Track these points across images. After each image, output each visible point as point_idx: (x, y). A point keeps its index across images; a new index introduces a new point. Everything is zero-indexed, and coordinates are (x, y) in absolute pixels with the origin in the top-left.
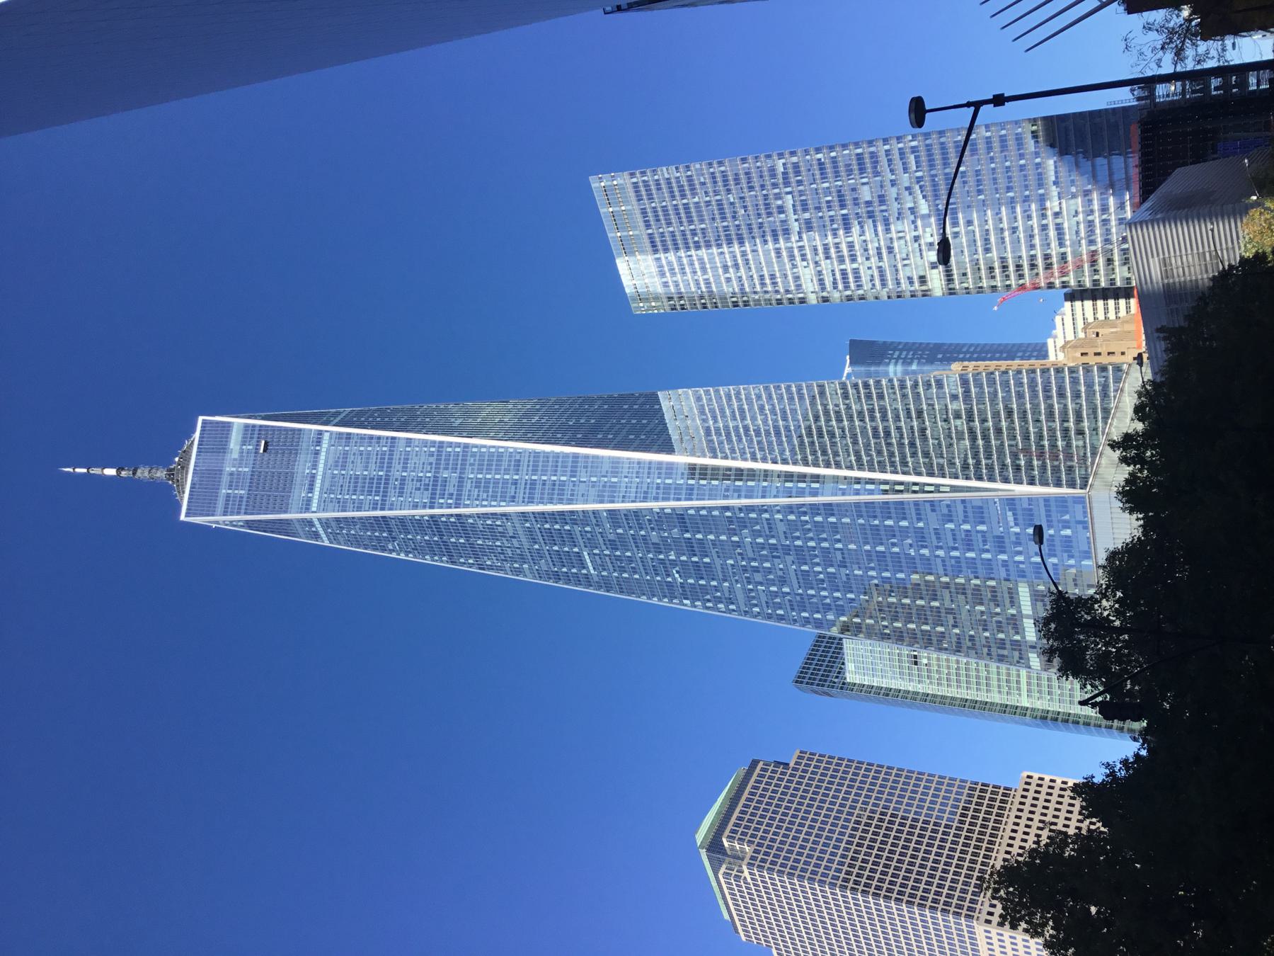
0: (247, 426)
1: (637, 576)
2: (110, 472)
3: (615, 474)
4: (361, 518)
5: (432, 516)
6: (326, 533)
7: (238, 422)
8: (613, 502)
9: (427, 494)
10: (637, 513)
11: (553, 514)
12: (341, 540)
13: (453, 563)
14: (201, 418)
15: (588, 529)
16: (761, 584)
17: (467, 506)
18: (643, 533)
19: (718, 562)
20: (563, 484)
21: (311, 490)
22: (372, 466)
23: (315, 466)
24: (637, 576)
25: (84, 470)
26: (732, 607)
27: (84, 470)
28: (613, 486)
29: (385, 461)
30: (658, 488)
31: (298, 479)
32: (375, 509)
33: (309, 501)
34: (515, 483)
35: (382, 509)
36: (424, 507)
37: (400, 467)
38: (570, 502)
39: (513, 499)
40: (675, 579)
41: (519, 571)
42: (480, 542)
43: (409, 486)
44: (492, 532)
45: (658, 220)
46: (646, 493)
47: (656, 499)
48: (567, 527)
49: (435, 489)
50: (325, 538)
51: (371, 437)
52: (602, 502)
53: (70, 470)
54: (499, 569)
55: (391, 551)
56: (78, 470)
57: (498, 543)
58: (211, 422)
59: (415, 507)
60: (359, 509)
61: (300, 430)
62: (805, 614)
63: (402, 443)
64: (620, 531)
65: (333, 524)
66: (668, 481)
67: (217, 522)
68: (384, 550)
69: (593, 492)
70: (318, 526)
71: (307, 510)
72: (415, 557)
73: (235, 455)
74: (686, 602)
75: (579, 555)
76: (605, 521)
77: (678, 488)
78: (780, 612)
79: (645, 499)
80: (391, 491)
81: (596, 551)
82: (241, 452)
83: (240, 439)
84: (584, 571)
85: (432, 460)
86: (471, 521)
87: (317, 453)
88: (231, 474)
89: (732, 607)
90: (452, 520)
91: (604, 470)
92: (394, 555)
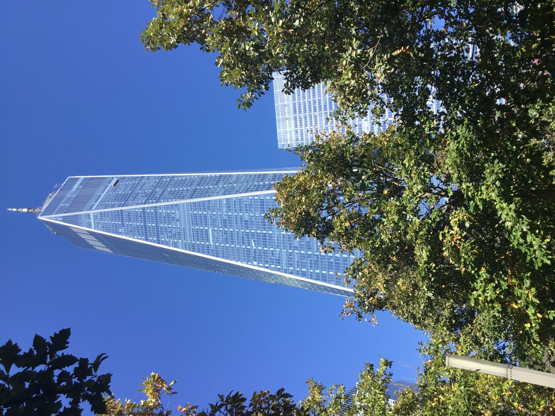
0: (85, 178)
1: (233, 246)
2: (25, 210)
3: (236, 182)
4: (111, 212)
5: (144, 209)
6: (94, 222)
8: (230, 194)
9: (146, 198)
10: (240, 200)
11: (199, 203)
12: (100, 226)
13: (147, 240)
15: (214, 213)
16: (296, 248)
17: (160, 202)
18: (241, 214)
19: (277, 233)
20: (209, 189)
21: (96, 202)
22: (128, 189)
24: (233, 246)
25: (15, 210)
26: (279, 267)
27: (15, 210)
28: (233, 187)
29: (134, 187)
30: (255, 186)
31: (95, 197)
32: (119, 206)
33: (93, 205)
34: (187, 190)
35: (123, 206)
36: (141, 204)
37: (139, 188)
38: (209, 196)
39: (183, 198)
40: (252, 246)
41: (176, 245)
42: (162, 225)
43: (141, 195)
44: (169, 218)
45: (299, 95)
46: (248, 188)
47: (252, 191)
48: (205, 213)
49: (150, 197)
50: (93, 226)
51: (133, 177)
52: (225, 194)
54: (167, 244)
55: (120, 233)
57: (170, 226)
58: (72, 178)
59: (137, 204)
60: (112, 207)
62: (317, 271)
63: (145, 179)
64: (230, 214)
65: (99, 217)
66: (261, 183)
68: (117, 233)
69: (223, 190)
70: (92, 218)
71: (90, 209)
72: (130, 237)
73: (73, 190)
74: (255, 263)
75: (207, 231)
76: (224, 205)
77: (265, 185)
78: (304, 270)
79: (247, 192)
80: (131, 199)
81: (216, 229)
82: (77, 189)
84: (207, 243)
85: (155, 184)
86: (160, 211)
87: (107, 186)
89: (279, 267)
90: (152, 211)
91: (233, 180)
92: (120, 237)
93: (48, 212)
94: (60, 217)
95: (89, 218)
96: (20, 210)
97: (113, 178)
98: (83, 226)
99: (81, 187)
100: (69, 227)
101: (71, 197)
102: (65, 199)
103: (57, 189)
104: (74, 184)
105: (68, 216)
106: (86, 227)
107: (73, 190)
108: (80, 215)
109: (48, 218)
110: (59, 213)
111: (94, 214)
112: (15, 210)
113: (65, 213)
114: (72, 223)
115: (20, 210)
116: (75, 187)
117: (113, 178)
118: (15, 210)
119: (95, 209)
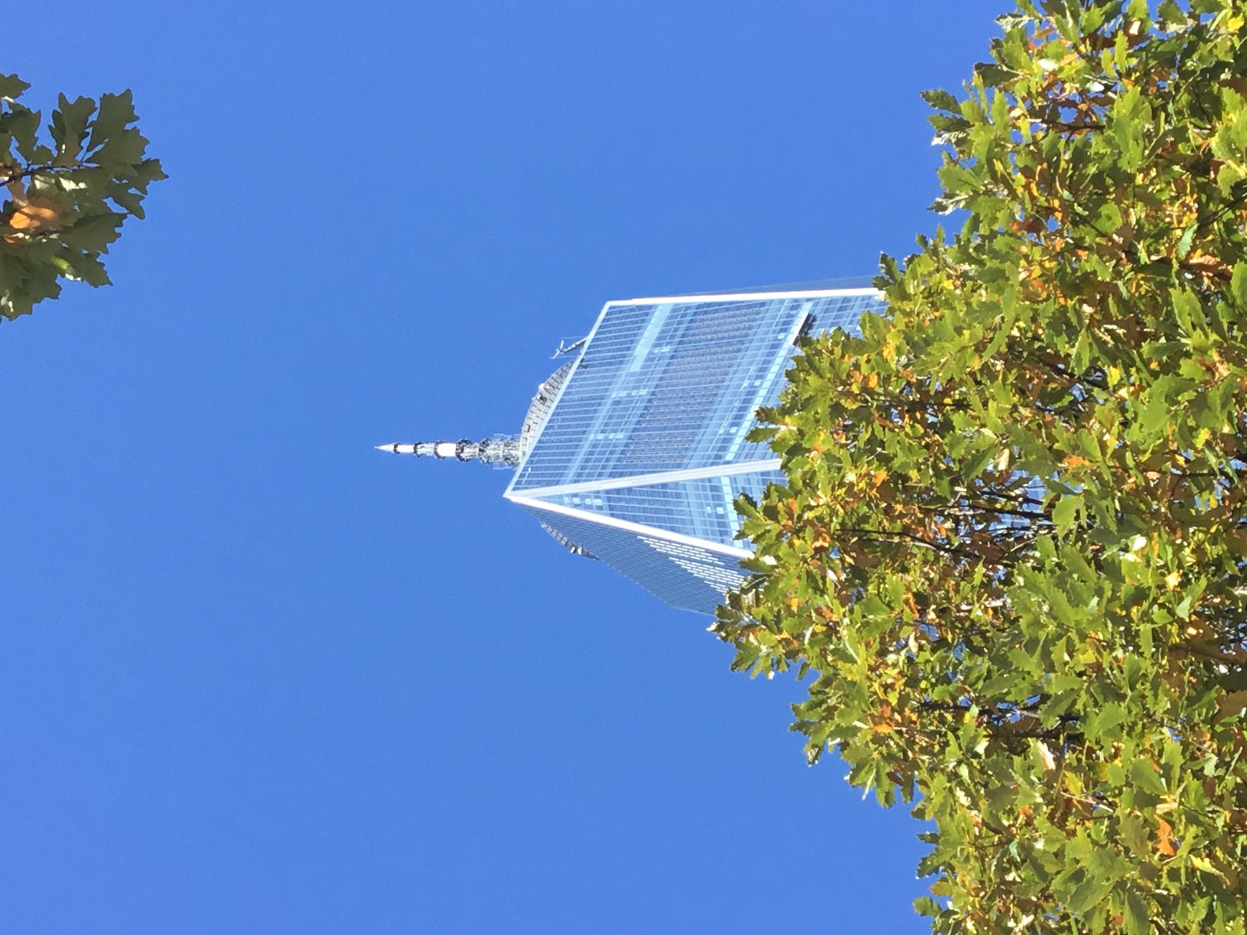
0: (676, 308)
2: (448, 450)
7: (665, 303)
14: (609, 304)
23: (762, 373)
31: (728, 400)
33: (728, 440)
53: (389, 448)
56: (401, 449)
58: (621, 310)
61: (763, 304)
67: (558, 499)
71: (717, 460)
73: (636, 366)
82: (650, 359)
83: (656, 335)
88: (617, 403)
93: (545, 469)
94: (597, 494)
95: (718, 498)
96: (427, 449)
97: (796, 305)
98: (693, 533)
99: (666, 349)
100: (633, 535)
101: (630, 400)
102: (604, 411)
103: (565, 362)
104: (631, 342)
105: (629, 490)
106: (706, 535)
107: (636, 366)
108: (676, 484)
109: (549, 499)
110: (589, 478)
111: (733, 480)
112: (406, 449)
113: (612, 475)
114: (648, 521)
115: (427, 449)
116: (641, 350)
117: (796, 305)
118: (406, 449)
119: (738, 457)
